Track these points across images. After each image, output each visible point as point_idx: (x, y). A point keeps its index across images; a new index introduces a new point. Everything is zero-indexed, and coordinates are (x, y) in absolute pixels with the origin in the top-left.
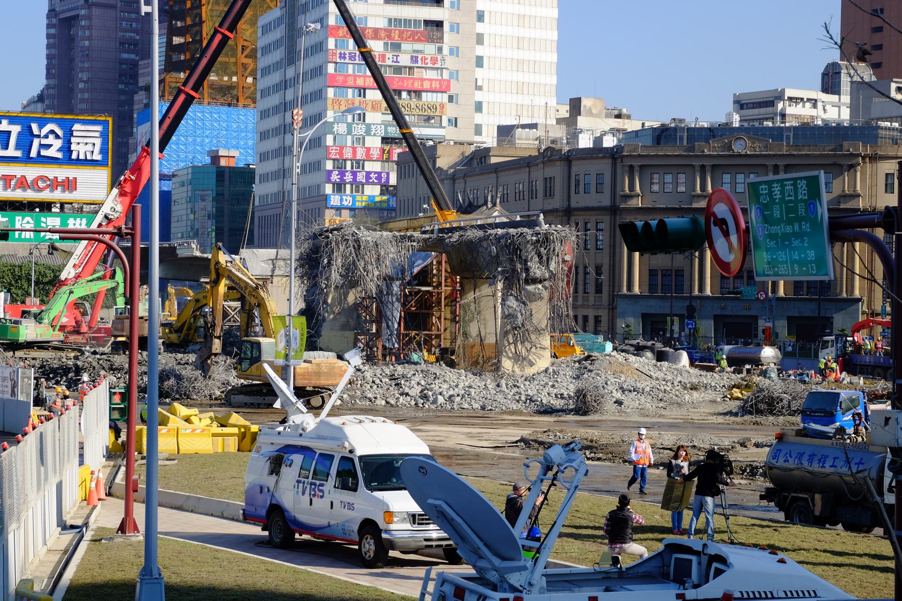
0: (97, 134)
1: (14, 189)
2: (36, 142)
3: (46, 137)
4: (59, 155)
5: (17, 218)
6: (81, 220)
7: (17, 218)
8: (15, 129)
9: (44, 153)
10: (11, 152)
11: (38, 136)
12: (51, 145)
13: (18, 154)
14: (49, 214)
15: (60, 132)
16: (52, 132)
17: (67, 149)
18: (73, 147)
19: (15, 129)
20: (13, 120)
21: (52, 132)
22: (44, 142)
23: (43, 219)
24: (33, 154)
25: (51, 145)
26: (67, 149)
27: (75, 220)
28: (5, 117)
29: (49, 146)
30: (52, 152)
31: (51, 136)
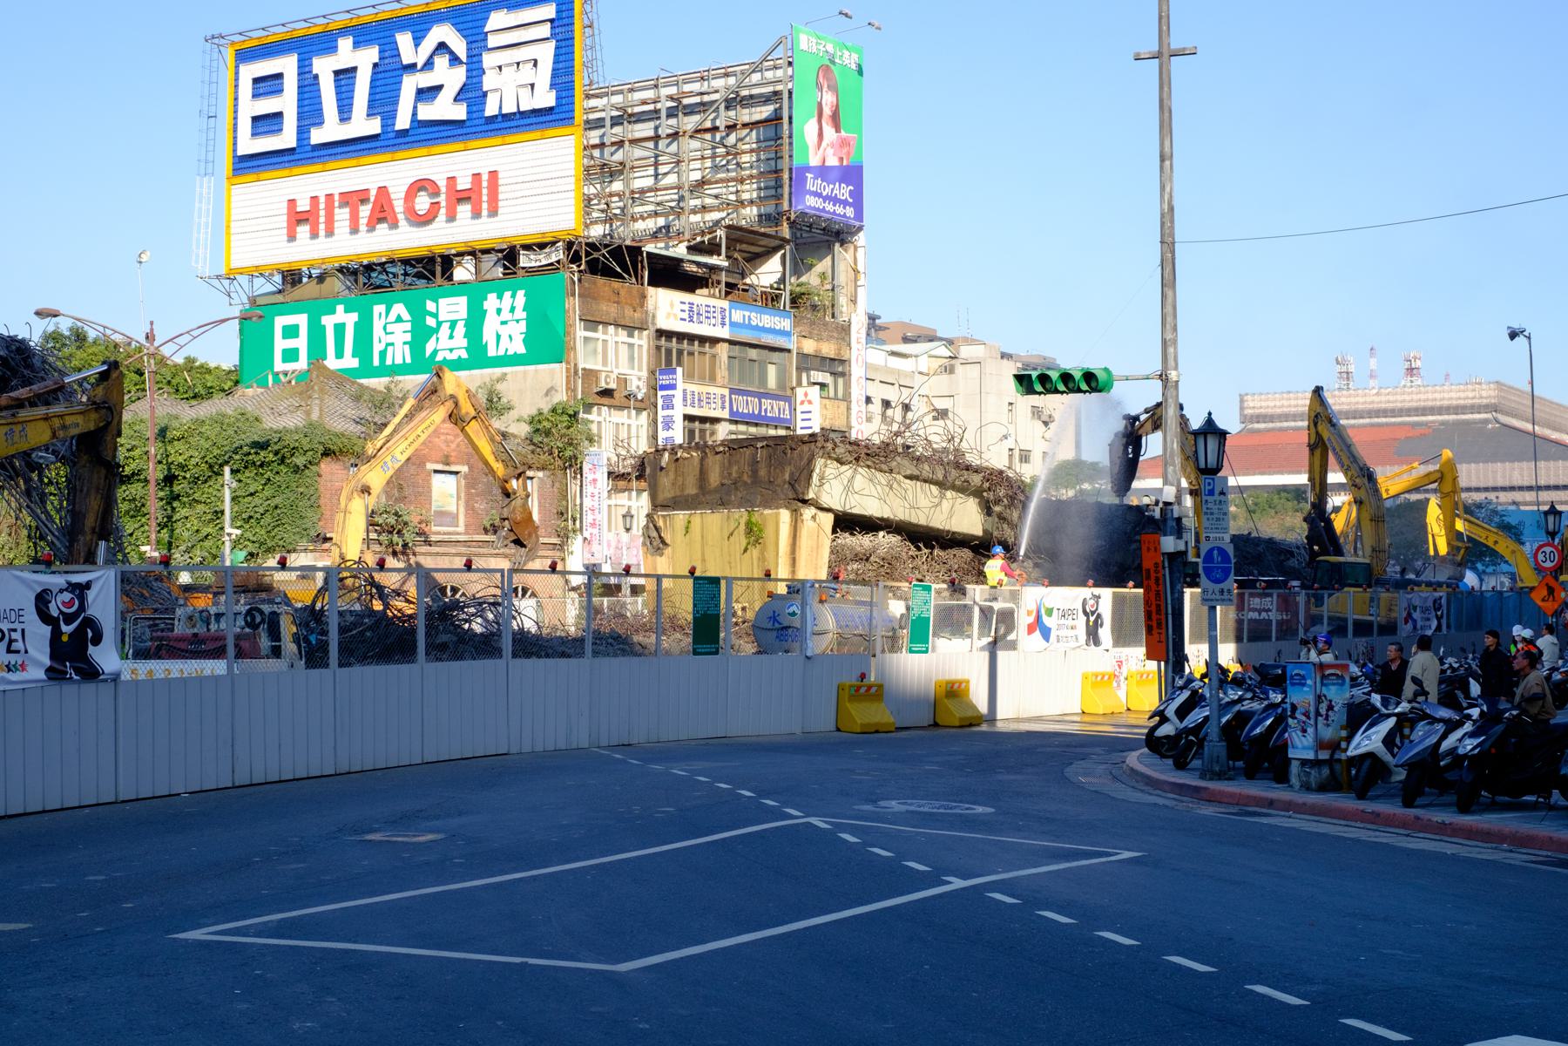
0: (545, 31)
1: (371, 227)
2: (410, 84)
3: (429, 64)
4: (459, 112)
5: (379, 309)
6: (513, 296)
7: (379, 309)
8: (366, 58)
9: (427, 112)
10: (363, 125)
11: (412, 67)
12: (439, 88)
13: (374, 127)
14: (447, 286)
15: (459, 46)
16: (442, 47)
17: (472, 93)
18: (489, 81)
19: (366, 58)
20: (362, 34)
21: (442, 47)
22: (425, 80)
23: (430, 306)
24: (403, 122)
25: (439, 88)
26: (472, 93)
27: (500, 297)
28: (344, 31)
29: (435, 90)
30: (446, 108)
31: (442, 62)
